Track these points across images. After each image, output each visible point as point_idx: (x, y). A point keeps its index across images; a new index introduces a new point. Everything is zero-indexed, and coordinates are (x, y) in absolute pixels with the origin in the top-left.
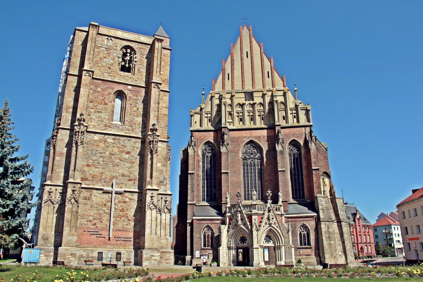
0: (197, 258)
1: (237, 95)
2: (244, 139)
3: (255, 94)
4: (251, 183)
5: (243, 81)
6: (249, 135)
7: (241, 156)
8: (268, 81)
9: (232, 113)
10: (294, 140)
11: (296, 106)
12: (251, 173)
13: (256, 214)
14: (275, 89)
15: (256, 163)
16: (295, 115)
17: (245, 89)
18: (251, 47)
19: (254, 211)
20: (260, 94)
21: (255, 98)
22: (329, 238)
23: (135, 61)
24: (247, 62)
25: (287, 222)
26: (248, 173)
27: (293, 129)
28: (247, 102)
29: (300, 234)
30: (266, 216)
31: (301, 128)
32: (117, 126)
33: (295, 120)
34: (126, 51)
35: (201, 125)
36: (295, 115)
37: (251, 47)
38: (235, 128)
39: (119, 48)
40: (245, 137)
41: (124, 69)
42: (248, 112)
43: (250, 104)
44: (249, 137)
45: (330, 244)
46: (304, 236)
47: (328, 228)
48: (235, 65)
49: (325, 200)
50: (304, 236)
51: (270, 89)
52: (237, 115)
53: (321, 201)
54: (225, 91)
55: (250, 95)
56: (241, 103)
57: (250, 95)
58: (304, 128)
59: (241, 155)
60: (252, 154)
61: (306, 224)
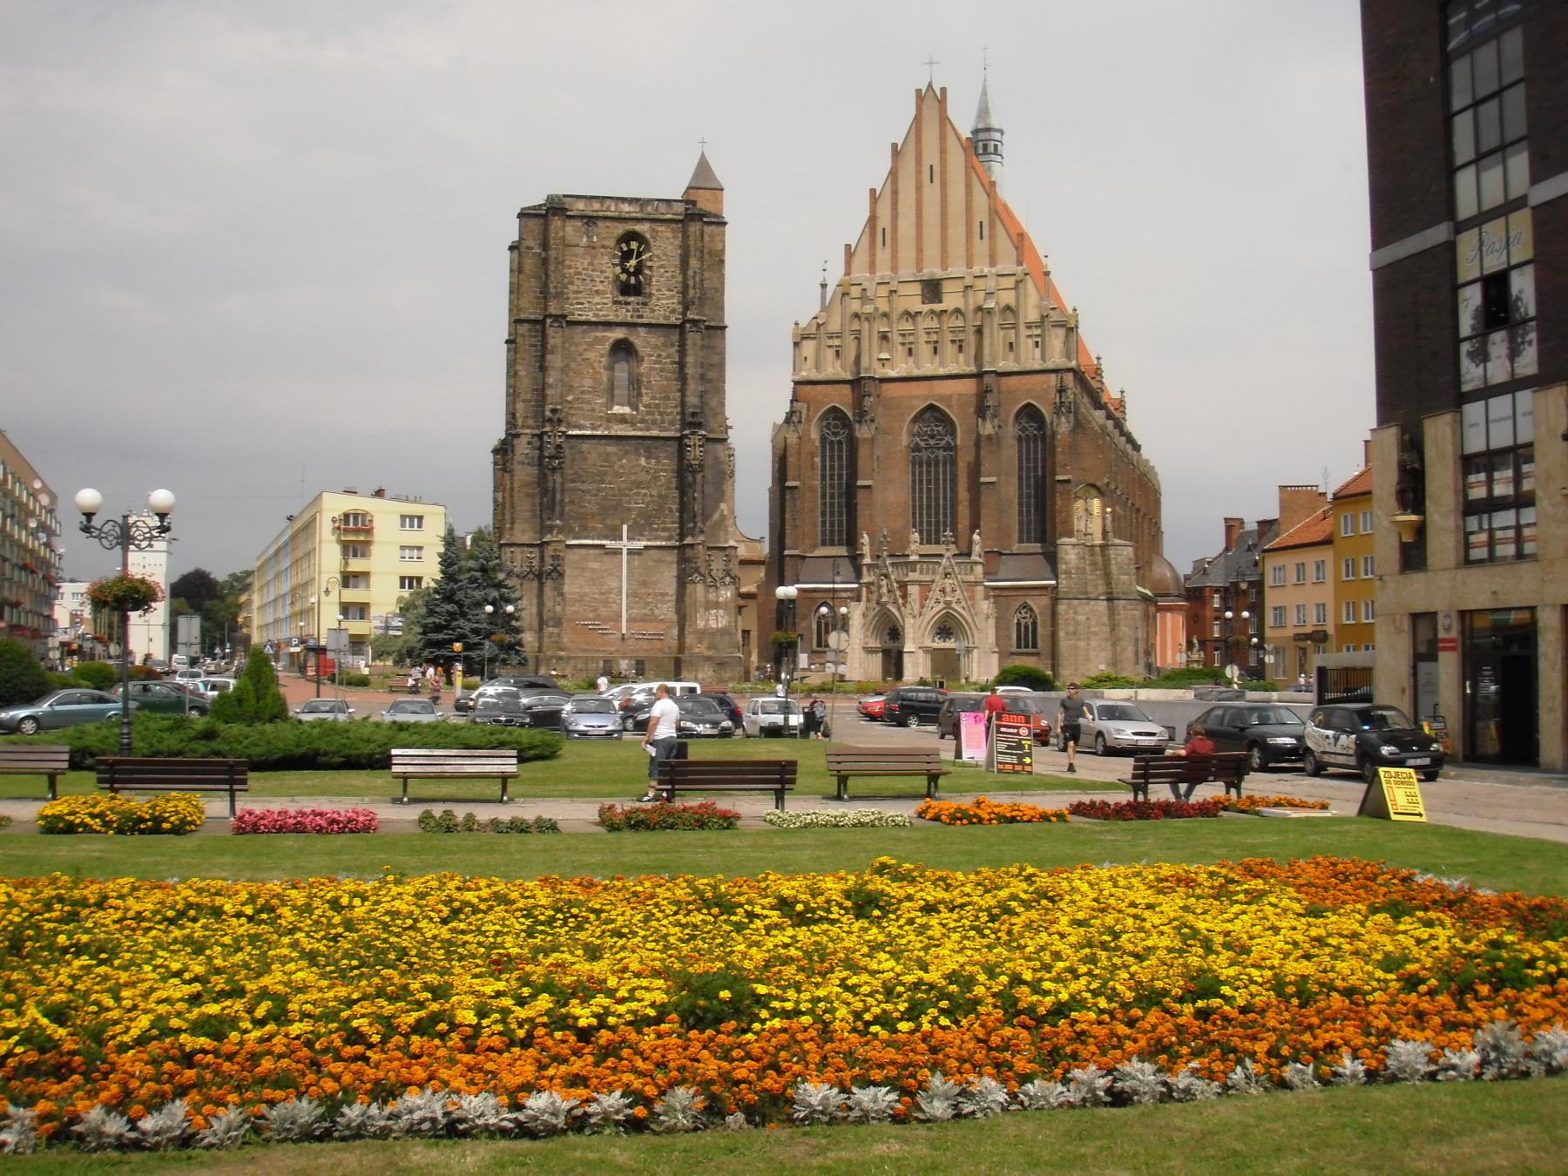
0: (804, 670)
1: (903, 289)
2: (916, 402)
3: (947, 287)
4: (929, 506)
5: (920, 250)
6: (925, 392)
7: (905, 443)
8: (981, 247)
9: (889, 335)
10: (1029, 405)
11: (1044, 318)
12: (929, 482)
13: (913, 582)
14: (994, 270)
15: (941, 458)
16: (1039, 339)
17: (925, 271)
18: (943, 152)
19: (913, 576)
20: (959, 286)
21: (945, 297)
22: (1074, 634)
23: (650, 268)
24: (931, 193)
25: (987, 597)
26: (921, 481)
27: (1028, 377)
28: (926, 308)
29: (1019, 624)
30: (936, 587)
31: (1048, 375)
32: (622, 419)
33: (1038, 352)
34: (628, 245)
35: (817, 366)
36: (1039, 339)
37: (943, 152)
38: (893, 374)
39: (611, 243)
40: (917, 397)
41: (626, 289)
42: (928, 333)
43: (933, 312)
44: (926, 398)
45: (1076, 647)
46: (1026, 628)
47: (1075, 613)
48: (900, 205)
49: (1076, 551)
50: (1026, 628)
51: (982, 270)
52: (900, 340)
53: (1067, 554)
54: (873, 279)
55: (932, 289)
56: (912, 310)
57: (932, 289)
58: (1053, 377)
59: (905, 439)
60: (932, 437)
61: (1030, 602)
